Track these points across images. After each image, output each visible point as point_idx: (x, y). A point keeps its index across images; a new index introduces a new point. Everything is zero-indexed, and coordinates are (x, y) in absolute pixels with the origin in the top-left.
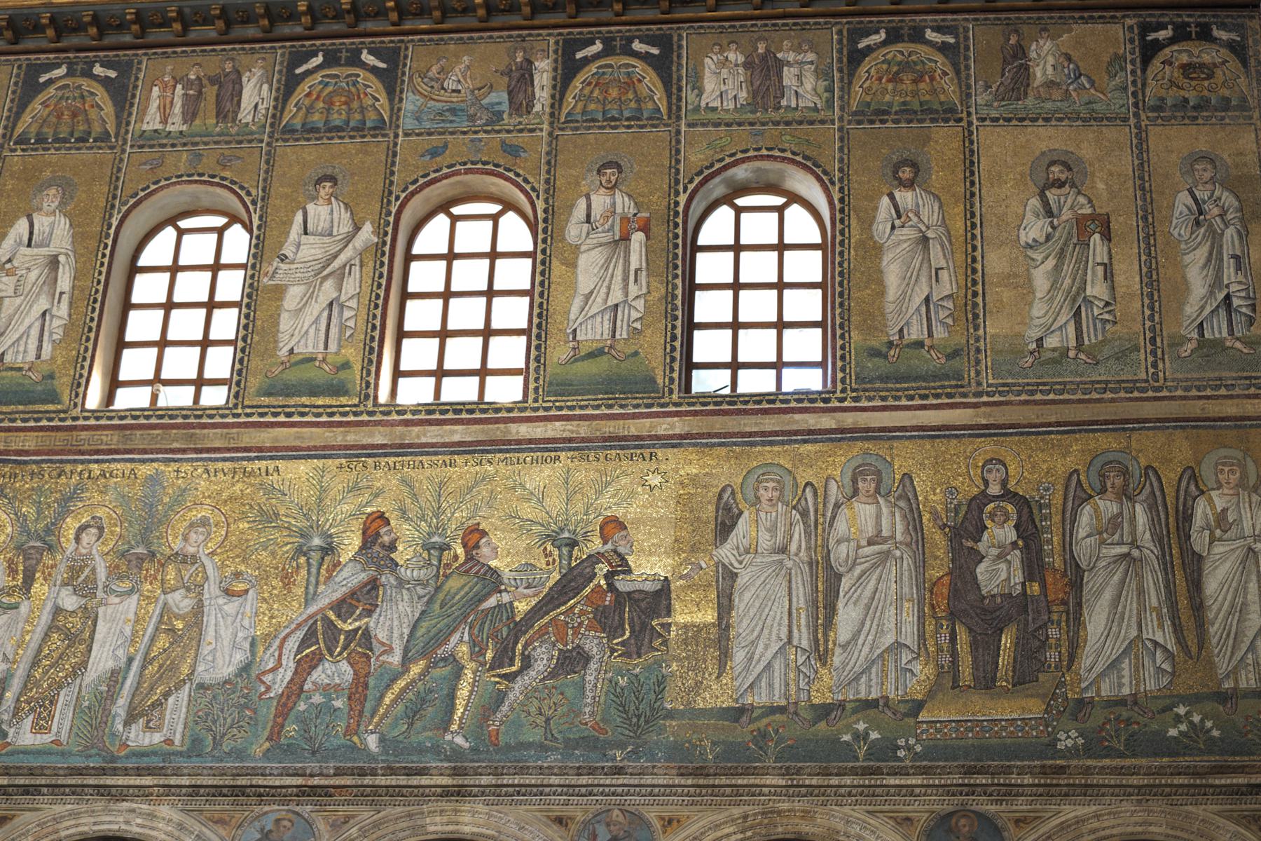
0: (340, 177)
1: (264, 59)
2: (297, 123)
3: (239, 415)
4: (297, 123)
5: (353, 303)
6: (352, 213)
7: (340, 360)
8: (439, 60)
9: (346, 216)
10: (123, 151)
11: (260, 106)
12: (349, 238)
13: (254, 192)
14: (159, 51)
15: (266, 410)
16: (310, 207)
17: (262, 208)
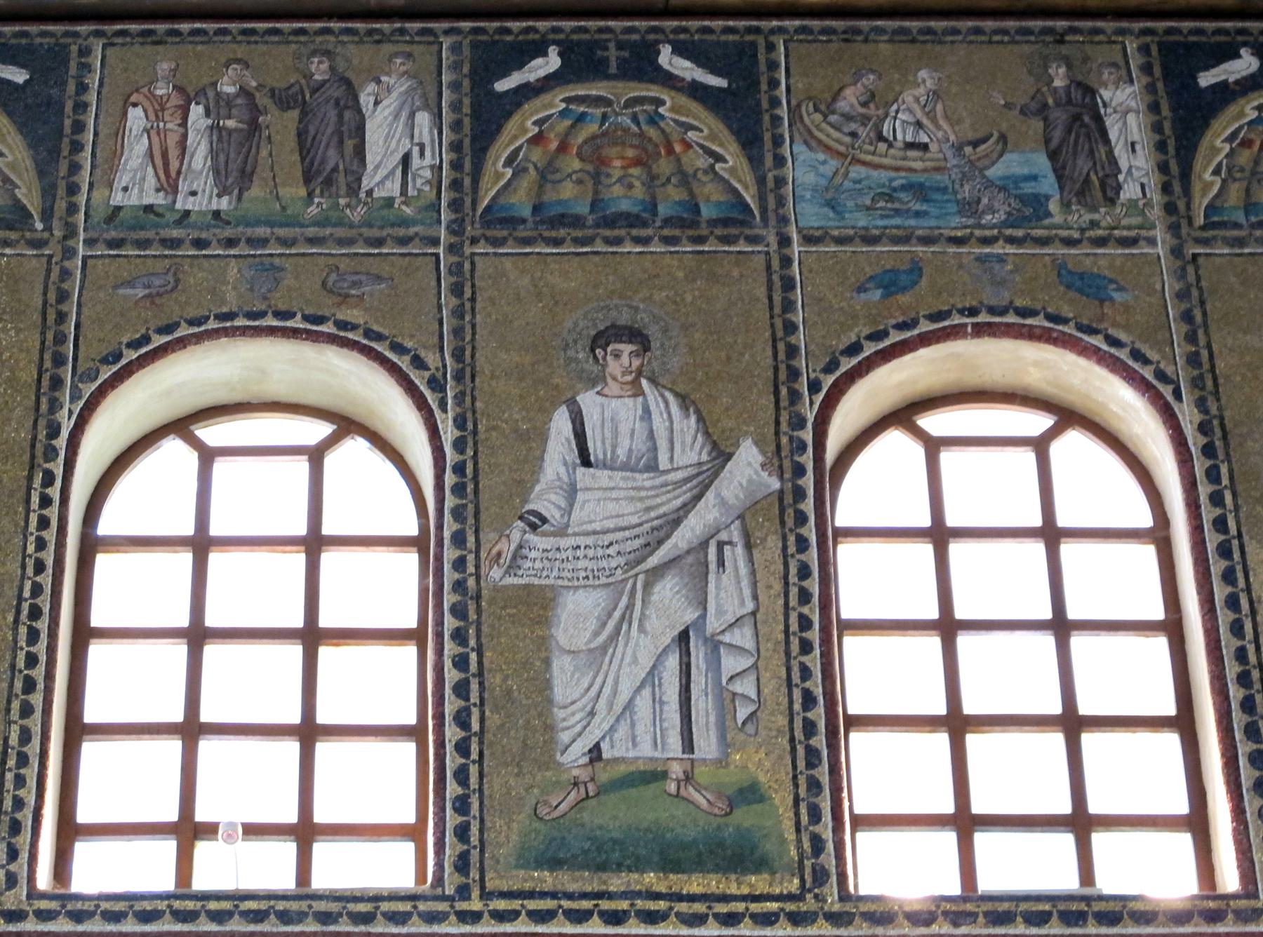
0: (653, 331)
1: (409, 56)
2: (521, 200)
3: (475, 917)
4: (521, 200)
5: (743, 637)
6: (700, 419)
7: (731, 778)
8: (857, 77)
9: (687, 426)
10: (69, 253)
11: (416, 162)
12: (704, 479)
13: (431, 359)
14: (134, 27)
15: (549, 904)
16: (588, 401)
17: (460, 398)
